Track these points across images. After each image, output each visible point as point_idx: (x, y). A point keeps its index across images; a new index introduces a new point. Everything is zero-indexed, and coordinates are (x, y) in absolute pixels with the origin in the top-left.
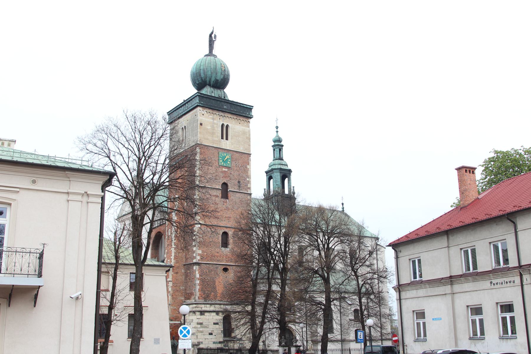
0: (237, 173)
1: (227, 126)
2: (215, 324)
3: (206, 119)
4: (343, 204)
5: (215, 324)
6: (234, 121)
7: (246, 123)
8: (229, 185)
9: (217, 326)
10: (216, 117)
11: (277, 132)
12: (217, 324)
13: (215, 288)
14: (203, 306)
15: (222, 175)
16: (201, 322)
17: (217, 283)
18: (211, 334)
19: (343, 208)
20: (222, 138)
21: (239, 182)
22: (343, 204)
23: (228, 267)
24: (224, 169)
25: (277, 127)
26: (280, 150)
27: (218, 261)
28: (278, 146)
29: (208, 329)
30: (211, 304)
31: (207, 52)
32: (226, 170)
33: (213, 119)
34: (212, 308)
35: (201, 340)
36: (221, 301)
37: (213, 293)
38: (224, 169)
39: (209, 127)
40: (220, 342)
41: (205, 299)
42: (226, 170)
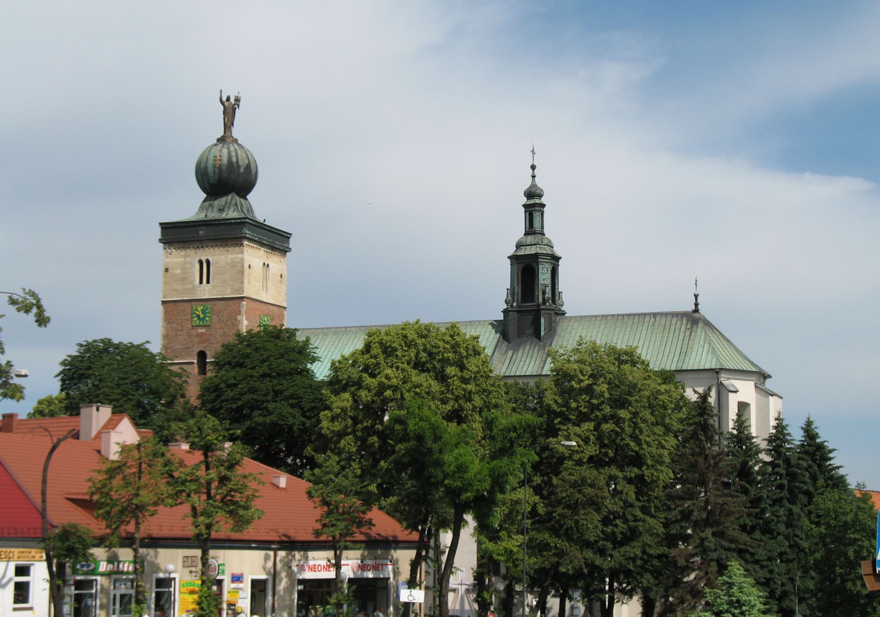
0: (220, 332)
1: (208, 262)
3: (176, 260)
4: (696, 296)
6: (217, 251)
7: (237, 249)
8: (208, 352)
10: (191, 252)
11: (534, 177)
15: (196, 340)
19: (696, 305)
20: (201, 282)
22: (696, 296)
24: (200, 331)
25: (533, 167)
26: (542, 214)
28: (534, 205)
31: (221, 133)
32: (203, 330)
33: (186, 256)
38: (200, 331)
39: (178, 272)
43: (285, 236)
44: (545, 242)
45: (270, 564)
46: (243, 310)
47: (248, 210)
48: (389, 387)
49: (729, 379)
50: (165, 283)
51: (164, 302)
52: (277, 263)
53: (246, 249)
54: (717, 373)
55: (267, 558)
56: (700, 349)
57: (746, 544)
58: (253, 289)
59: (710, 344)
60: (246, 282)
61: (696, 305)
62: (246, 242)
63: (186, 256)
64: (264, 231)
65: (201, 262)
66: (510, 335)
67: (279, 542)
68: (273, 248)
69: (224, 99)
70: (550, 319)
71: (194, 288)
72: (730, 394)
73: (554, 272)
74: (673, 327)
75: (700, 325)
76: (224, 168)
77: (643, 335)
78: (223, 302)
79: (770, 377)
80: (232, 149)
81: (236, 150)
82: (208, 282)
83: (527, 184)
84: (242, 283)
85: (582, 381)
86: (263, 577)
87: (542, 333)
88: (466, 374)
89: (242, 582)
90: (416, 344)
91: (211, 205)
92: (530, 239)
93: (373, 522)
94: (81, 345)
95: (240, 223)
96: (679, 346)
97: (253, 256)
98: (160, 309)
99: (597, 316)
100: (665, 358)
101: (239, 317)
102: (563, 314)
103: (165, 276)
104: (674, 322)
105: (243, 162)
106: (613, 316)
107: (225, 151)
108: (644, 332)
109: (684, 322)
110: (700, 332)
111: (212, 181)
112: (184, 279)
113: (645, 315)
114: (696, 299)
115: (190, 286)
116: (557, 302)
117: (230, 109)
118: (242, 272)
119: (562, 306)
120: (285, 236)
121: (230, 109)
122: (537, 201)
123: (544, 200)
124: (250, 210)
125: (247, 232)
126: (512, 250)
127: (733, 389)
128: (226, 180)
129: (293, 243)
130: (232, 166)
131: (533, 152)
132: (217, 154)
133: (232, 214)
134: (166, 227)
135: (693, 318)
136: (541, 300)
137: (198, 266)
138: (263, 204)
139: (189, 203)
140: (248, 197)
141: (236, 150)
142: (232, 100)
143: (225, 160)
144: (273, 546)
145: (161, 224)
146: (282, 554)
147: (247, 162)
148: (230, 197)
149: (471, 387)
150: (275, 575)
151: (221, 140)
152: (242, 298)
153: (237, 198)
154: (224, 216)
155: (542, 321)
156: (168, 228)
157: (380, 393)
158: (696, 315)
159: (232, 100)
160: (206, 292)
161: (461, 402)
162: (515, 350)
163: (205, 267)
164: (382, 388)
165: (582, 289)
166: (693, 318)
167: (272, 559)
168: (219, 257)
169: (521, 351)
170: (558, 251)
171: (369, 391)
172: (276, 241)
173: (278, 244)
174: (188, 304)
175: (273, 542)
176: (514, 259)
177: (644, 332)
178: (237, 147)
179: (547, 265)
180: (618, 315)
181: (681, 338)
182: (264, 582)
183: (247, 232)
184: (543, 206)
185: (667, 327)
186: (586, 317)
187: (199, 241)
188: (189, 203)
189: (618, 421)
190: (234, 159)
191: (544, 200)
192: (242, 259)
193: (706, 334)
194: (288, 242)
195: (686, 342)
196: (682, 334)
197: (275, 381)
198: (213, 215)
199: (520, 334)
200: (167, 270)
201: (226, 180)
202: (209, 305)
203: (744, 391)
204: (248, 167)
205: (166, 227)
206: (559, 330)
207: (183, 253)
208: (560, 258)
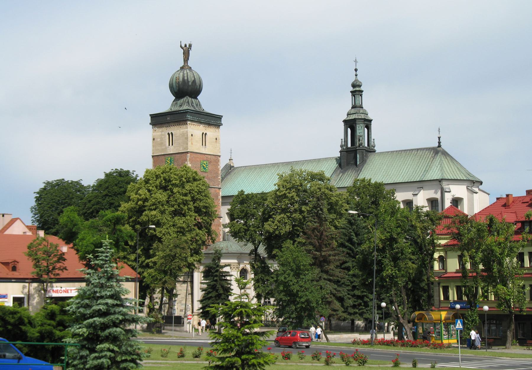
1: (172, 134)
4: (439, 138)
7: (185, 126)
10: (164, 129)
11: (356, 75)
19: (439, 143)
22: (439, 138)
25: (356, 70)
26: (361, 95)
28: (356, 91)
31: (182, 64)
43: (219, 118)
44: (361, 111)
45: (26, 290)
46: (188, 159)
47: (197, 105)
48: (141, 200)
49: (448, 185)
50: (153, 146)
51: (153, 156)
52: (211, 132)
53: (189, 126)
54: (440, 181)
55: (24, 287)
56: (436, 168)
57: (338, 277)
58: (195, 146)
59: (441, 165)
60: (190, 143)
61: (439, 143)
63: (162, 131)
64: (202, 116)
65: (169, 134)
66: (342, 164)
67: (31, 279)
68: (209, 124)
69: (183, 46)
70: (363, 155)
71: (166, 148)
72: (446, 193)
73: (368, 127)
74: (425, 156)
75: (439, 154)
76: (180, 83)
77: (409, 162)
78: (178, 155)
79: (481, 183)
80: (185, 72)
81: (187, 73)
83: (353, 79)
84: (187, 144)
85: (282, 191)
86: (22, 296)
87: (358, 163)
88: (184, 191)
89: (6, 298)
90: (160, 177)
91: (176, 103)
92: (353, 111)
93: (67, 268)
94: (44, 183)
95: (186, 112)
96: (425, 167)
97: (194, 130)
98: (151, 160)
99: (388, 152)
100: (416, 174)
102: (375, 151)
103: (153, 142)
104: (426, 153)
105: (191, 79)
106: (397, 151)
107: (181, 74)
108: (410, 159)
109: (432, 153)
110: (439, 157)
111: (176, 91)
112: (161, 144)
113: (412, 150)
114: (439, 140)
115: (164, 147)
116: (370, 146)
117: (187, 51)
118: (187, 138)
119: (374, 147)
120: (219, 118)
121: (187, 51)
122: (357, 89)
123: (362, 88)
124: (199, 104)
125: (189, 117)
126: (345, 117)
127: (447, 190)
128: (186, 89)
129: (223, 121)
130: (185, 82)
131: (356, 61)
132: (177, 76)
133: (185, 107)
134: (153, 116)
135: (437, 151)
136: (358, 144)
137: (168, 136)
138: (207, 102)
139: (165, 102)
140: (198, 97)
141: (187, 73)
142: (188, 46)
143: (181, 79)
144: (27, 281)
145: (150, 115)
146: (35, 285)
147: (193, 79)
148: (185, 98)
149: (188, 198)
150: (29, 296)
151: (182, 68)
152: (187, 152)
153: (190, 99)
154: (181, 109)
155: (358, 156)
157: (137, 204)
158: (439, 149)
159: (188, 46)
160: (171, 150)
161: (181, 206)
162: (343, 173)
163: (171, 135)
164: (139, 200)
165: (383, 136)
166: (437, 151)
167: (28, 288)
168: (177, 130)
169: (346, 173)
170: (370, 116)
171: (133, 201)
172: (213, 121)
173: (212, 122)
174: (164, 157)
175: (27, 279)
176: (345, 121)
177: (410, 159)
178: (188, 71)
179: (361, 125)
180: (399, 151)
181: (427, 162)
182: (23, 298)
183: (189, 117)
184: (362, 91)
185: (422, 157)
186: (383, 153)
187: (168, 123)
188: (165, 102)
189: (301, 212)
190: (186, 78)
191: (362, 88)
192: (187, 132)
193: (441, 159)
194: (221, 121)
195: (429, 164)
196: (429, 160)
197: (111, 198)
198: (174, 109)
199: (348, 164)
200: (154, 139)
201: (186, 89)
202: (173, 156)
203: (458, 191)
204: (194, 81)
205: (153, 116)
206: (368, 161)
207: (161, 130)
208: (372, 120)
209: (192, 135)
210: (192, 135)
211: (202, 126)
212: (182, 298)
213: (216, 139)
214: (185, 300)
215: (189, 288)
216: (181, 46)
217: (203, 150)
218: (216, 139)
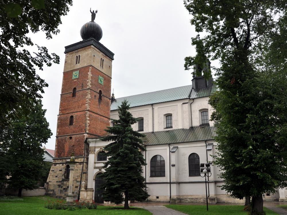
1: (79, 56)
2: (60, 171)
5: (60, 171)
9: (61, 172)
12: (61, 170)
13: (64, 150)
14: (57, 160)
16: (54, 170)
17: (65, 146)
18: (56, 177)
21: (82, 84)
23: (72, 136)
27: (67, 133)
29: (56, 174)
30: (61, 159)
32: (76, 80)
34: (61, 162)
35: (51, 180)
36: (67, 157)
37: (63, 153)
40: (60, 182)
41: (59, 157)
42: (76, 80)
46: (90, 70)
62: (92, 46)
69: (92, 11)
82: (79, 63)
87: (208, 85)
101: (88, 73)
111: (84, 33)
117: (93, 15)
121: (93, 15)
129: (114, 57)
156: (67, 48)
160: (79, 66)
205: (66, 48)
209: (94, 56)
210: (94, 56)
211: (101, 53)
212: (77, 176)
213: (110, 67)
214: (80, 178)
215: (84, 168)
216: (90, 11)
217: (100, 69)
218: (110, 67)
